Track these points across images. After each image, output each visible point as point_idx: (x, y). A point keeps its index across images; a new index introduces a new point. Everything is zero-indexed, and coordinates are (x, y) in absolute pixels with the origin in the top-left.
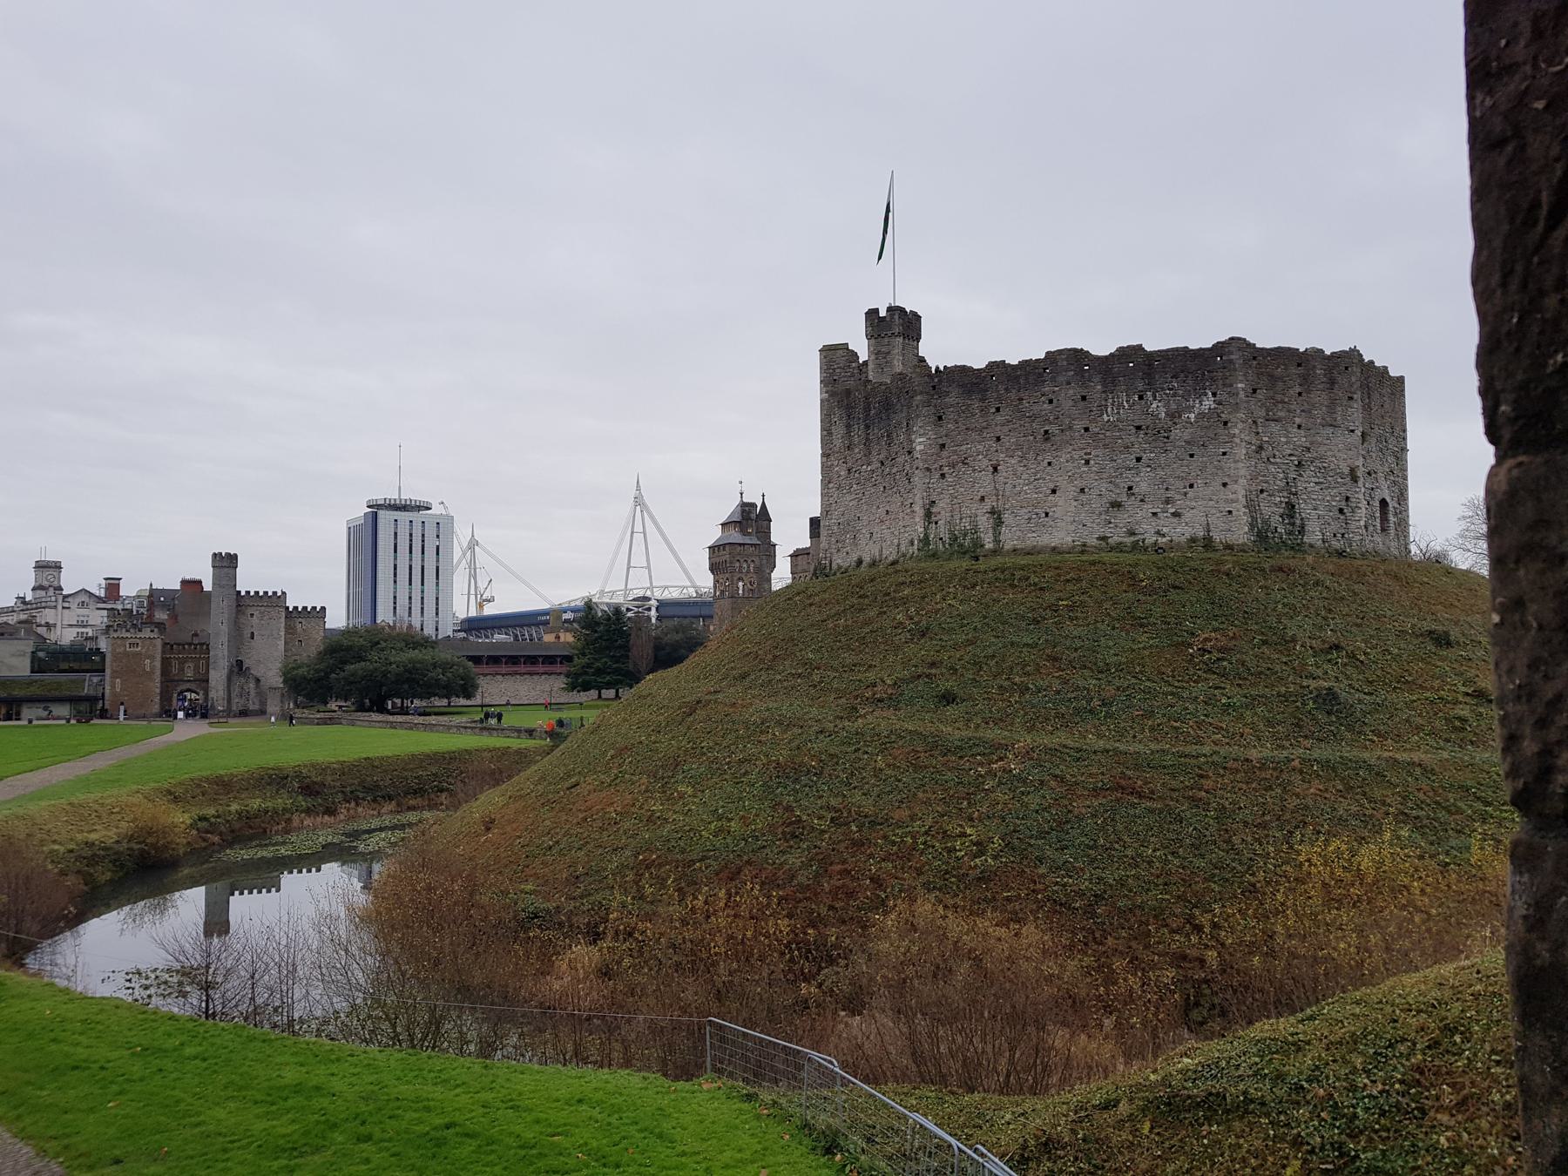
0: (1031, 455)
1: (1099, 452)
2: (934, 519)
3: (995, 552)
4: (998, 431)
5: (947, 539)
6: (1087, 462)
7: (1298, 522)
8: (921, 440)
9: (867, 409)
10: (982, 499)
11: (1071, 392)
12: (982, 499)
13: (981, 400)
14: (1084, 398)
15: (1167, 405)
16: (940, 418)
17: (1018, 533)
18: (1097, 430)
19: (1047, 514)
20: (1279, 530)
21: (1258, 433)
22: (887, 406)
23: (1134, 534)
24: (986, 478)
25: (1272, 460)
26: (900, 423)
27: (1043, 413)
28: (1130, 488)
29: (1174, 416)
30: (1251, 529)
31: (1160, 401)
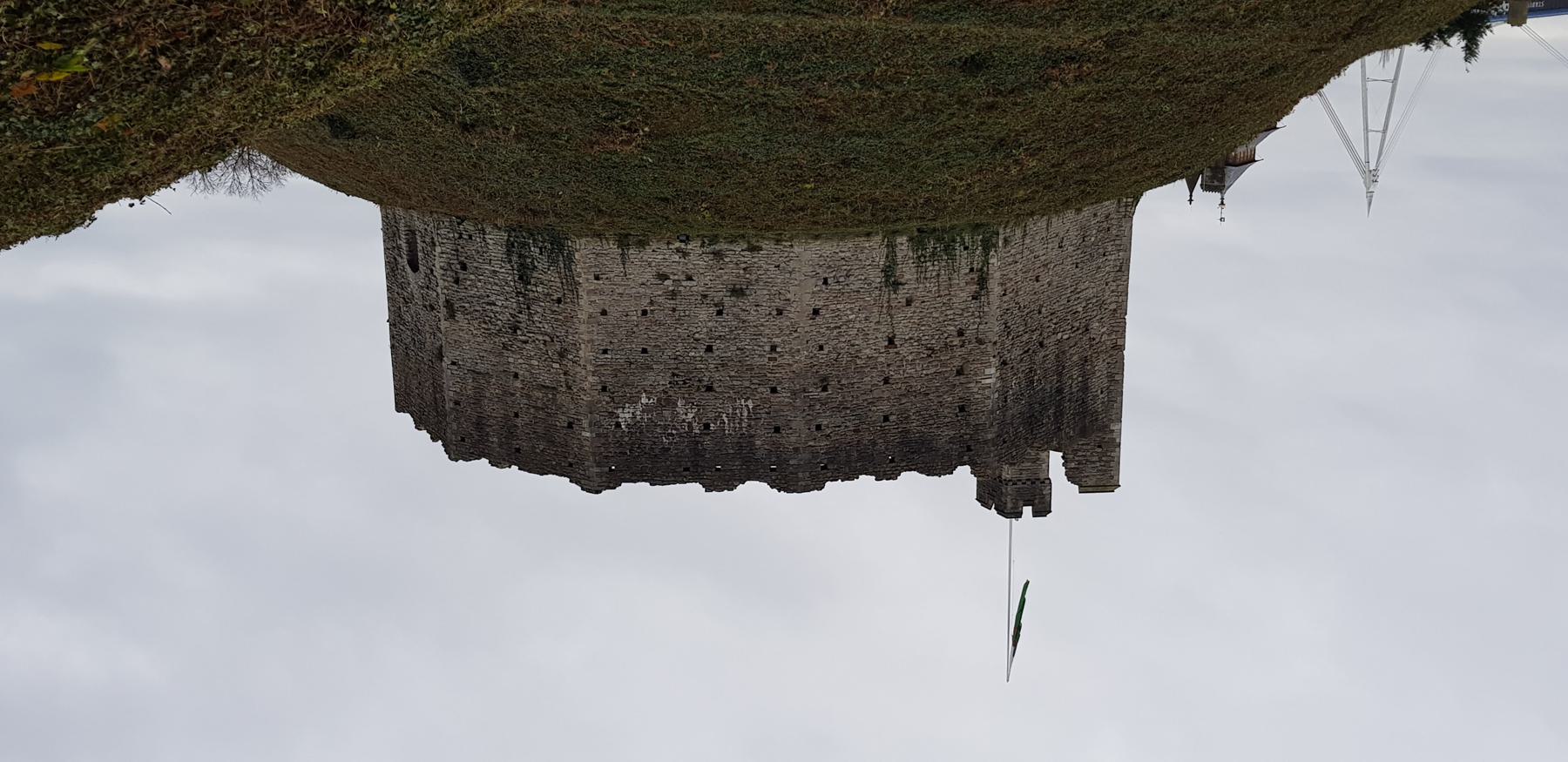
0: (845, 359)
1: (758, 361)
2: (975, 276)
7: (515, 258)
8: (988, 381)
9: (1059, 414)
10: (909, 302)
11: (793, 439)
12: (909, 302)
13: (908, 432)
15: (675, 415)
16: (962, 409)
19: (825, 282)
20: (538, 250)
21: (565, 374)
22: (1031, 420)
23: (713, 253)
24: (902, 331)
25: (547, 338)
26: (1017, 400)
27: (828, 413)
28: (720, 313)
29: (667, 402)
31: (684, 421)
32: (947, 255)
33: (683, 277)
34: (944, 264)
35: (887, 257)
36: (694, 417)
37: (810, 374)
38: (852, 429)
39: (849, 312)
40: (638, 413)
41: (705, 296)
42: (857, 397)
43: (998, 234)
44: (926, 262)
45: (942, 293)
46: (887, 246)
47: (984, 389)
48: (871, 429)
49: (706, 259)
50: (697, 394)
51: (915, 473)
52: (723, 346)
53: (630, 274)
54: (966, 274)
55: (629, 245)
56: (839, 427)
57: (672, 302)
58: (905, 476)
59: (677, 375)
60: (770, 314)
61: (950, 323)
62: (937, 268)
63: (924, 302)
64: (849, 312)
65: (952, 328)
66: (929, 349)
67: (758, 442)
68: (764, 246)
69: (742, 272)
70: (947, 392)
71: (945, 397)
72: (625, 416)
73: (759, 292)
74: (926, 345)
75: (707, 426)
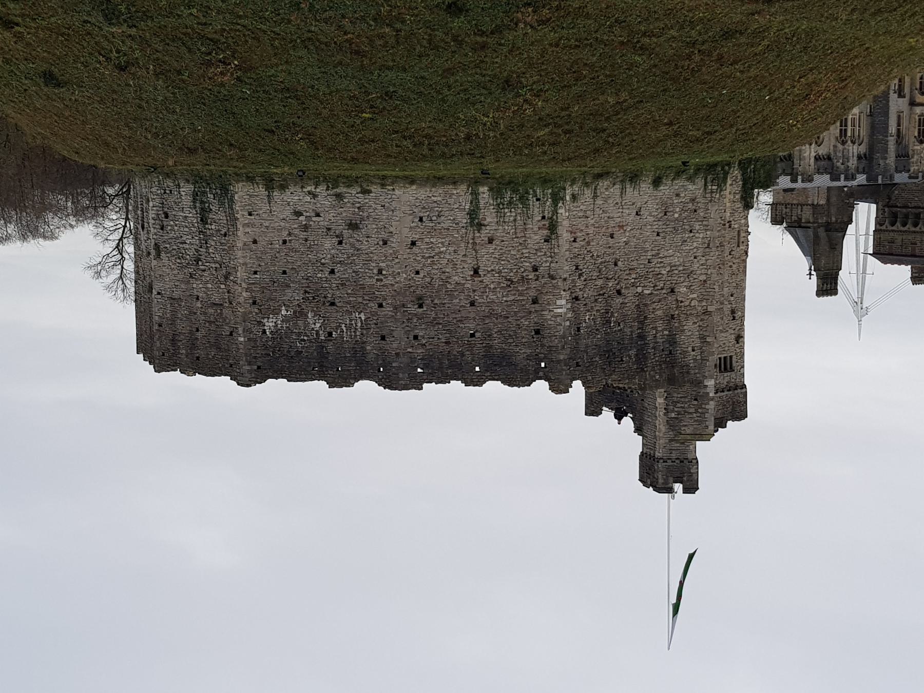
0: (437, 283)
1: (369, 282)
2: (547, 223)
3: (476, 182)
4: (471, 312)
5: (532, 200)
8: (559, 311)
10: (491, 241)
11: (395, 345)
12: (491, 241)
13: (491, 347)
15: (306, 325)
16: (537, 332)
17: (451, 201)
19: (421, 220)
23: (336, 195)
24: (485, 263)
27: (423, 326)
28: (340, 243)
29: (300, 314)
30: (233, 196)
31: (313, 329)
32: (522, 203)
33: (313, 214)
34: (519, 211)
35: (471, 203)
36: (320, 327)
37: (408, 293)
38: (444, 341)
39: (440, 245)
40: (279, 322)
41: (329, 229)
42: (448, 315)
43: (564, 189)
44: (504, 208)
46: (471, 194)
47: (556, 317)
48: (460, 342)
49: (330, 200)
50: (323, 308)
52: (342, 269)
53: (274, 211)
54: (539, 221)
55: (273, 188)
56: (433, 338)
57: (305, 233)
59: (309, 293)
60: (378, 244)
61: (525, 260)
62: (514, 214)
63: (503, 241)
64: (440, 245)
65: (528, 264)
66: (509, 280)
67: (368, 348)
68: (373, 190)
69: (356, 210)
70: (524, 317)
71: (521, 321)
72: (269, 324)
73: (369, 226)
74: (505, 277)
75: (330, 334)
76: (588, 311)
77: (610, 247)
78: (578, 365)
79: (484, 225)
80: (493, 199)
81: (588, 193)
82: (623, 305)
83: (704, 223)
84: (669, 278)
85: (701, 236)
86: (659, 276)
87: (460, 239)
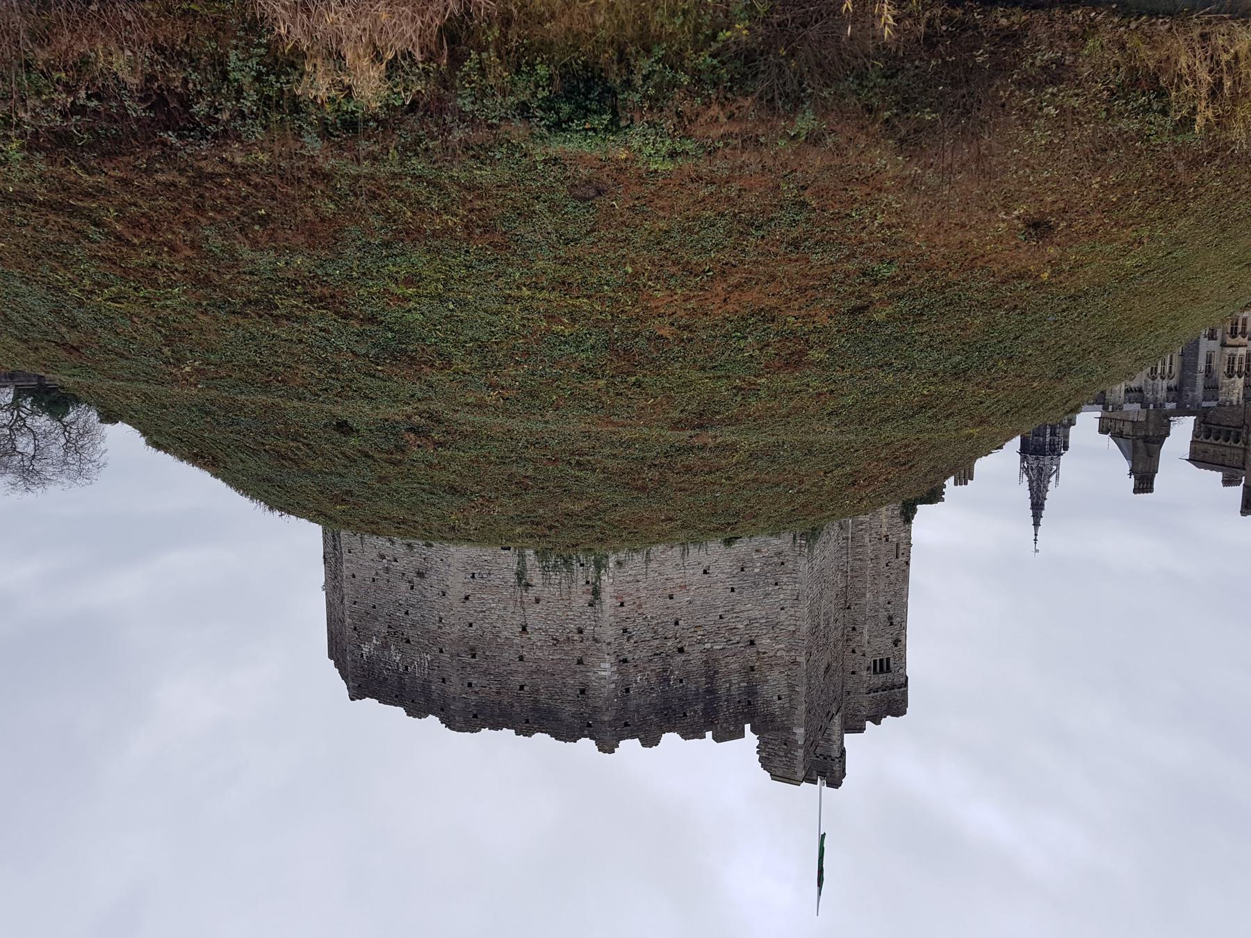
0: (489, 636)
2: (590, 587)
5: (576, 565)
6: (441, 619)
8: (603, 673)
10: (537, 601)
12: (537, 601)
13: (538, 701)
14: (444, 681)
16: (583, 692)
17: (500, 561)
18: (434, 648)
19: (473, 577)
24: (533, 623)
35: (518, 564)
37: (461, 643)
39: (491, 601)
43: (607, 557)
45: (564, 597)
51: (547, 736)
58: (538, 736)
64: (491, 601)
65: (572, 626)
76: (640, 672)
77: (668, 608)
78: (626, 725)
79: (531, 586)
80: (539, 561)
81: (639, 558)
82: (686, 663)
83: (793, 575)
84: (748, 632)
85: (790, 587)
86: (734, 631)
87: (509, 596)
